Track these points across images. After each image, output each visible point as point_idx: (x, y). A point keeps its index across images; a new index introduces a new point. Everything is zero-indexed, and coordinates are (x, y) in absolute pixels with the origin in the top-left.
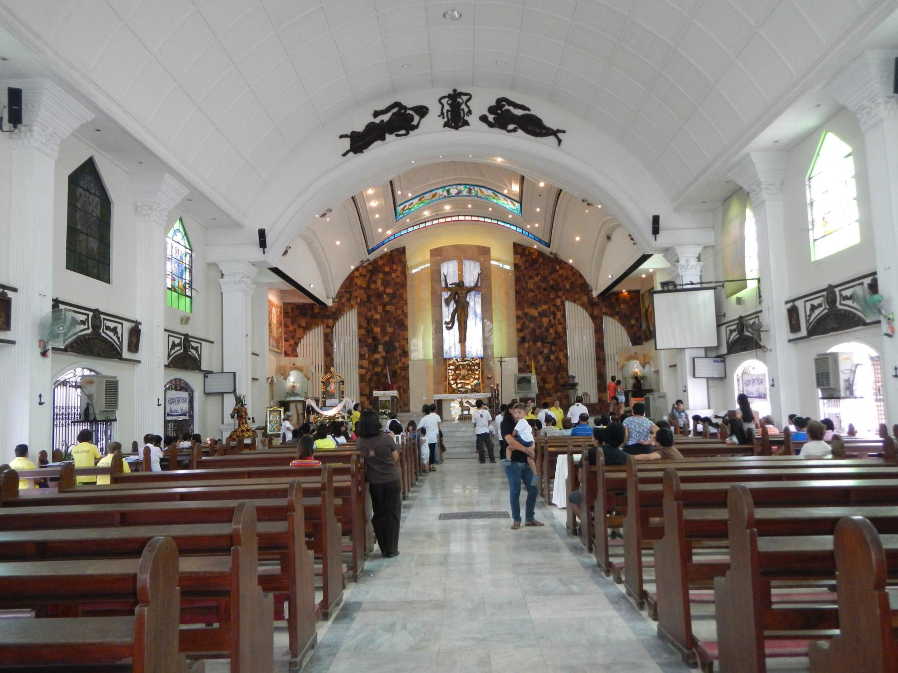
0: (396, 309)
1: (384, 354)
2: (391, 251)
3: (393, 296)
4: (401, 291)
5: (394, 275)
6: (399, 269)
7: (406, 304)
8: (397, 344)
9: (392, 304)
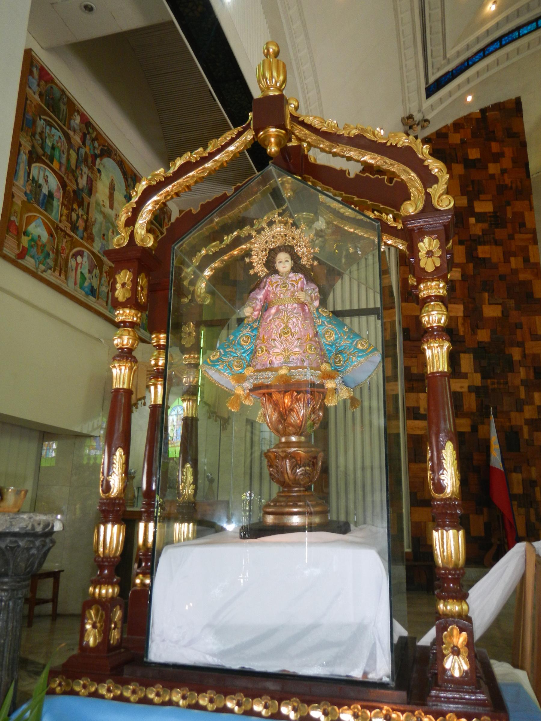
0: (507, 256)
1: (477, 379)
2: (483, 111)
3: (496, 220)
4: (519, 205)
5: (493, 169)
6: (508, 152)
7: (535, 242)
8: (516, 354)
9: (496, 243)
